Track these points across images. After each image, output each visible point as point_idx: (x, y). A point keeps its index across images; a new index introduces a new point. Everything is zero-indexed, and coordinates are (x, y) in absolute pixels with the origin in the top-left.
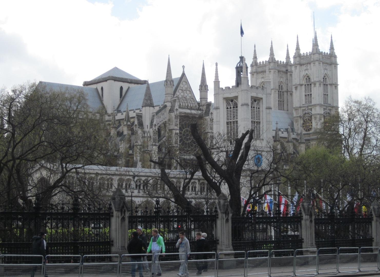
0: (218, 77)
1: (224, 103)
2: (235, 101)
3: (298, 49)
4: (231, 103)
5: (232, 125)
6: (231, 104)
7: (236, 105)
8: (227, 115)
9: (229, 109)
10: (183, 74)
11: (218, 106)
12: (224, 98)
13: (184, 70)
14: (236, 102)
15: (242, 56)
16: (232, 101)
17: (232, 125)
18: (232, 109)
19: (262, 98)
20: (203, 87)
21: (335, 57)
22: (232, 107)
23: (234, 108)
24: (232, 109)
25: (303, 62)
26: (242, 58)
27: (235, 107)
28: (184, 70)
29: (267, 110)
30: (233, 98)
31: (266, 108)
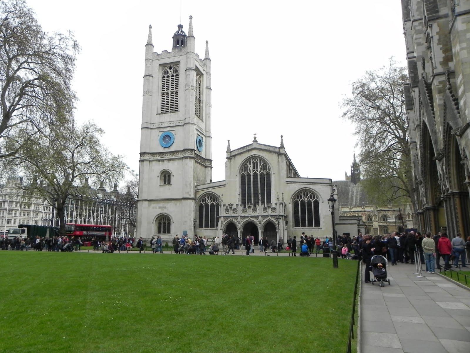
1: (159, 69)
4: (169, 70)
5: (170, 97)
6: (169, 72)
9: (166, 78)
11: (150, 73)
12: (160, 65)
15: (182, 24)
16: (170, 68)
17: (170, 97)
18: (170, 78)
19: (203, 75)
22: (170, 75)
23: (173, 76)
24: (170, 78)
26: (180, 27)
29: (207, 89)
31: (206, 88)
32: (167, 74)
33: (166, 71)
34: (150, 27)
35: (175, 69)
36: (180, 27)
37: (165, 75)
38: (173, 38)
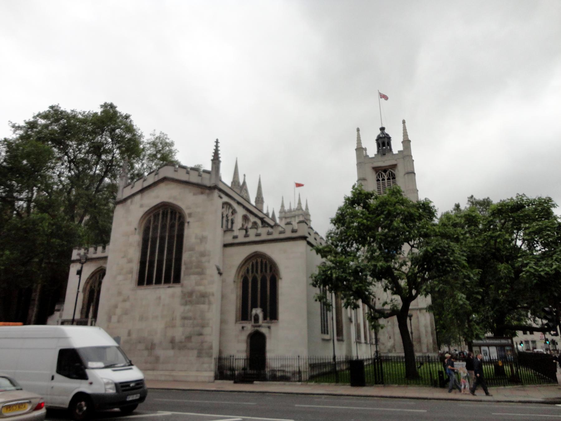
0: (361, 143)
2: (390, 171)
3: (283, 206)
4: (384, 174)
7: (392, 175)
8: (378, 189)
10: (244, 183)
13: (244, 178)
14: (392, 173)
15: (383, 126)
16: (385, 171)
18: (386, 180)
20: (260, 199)
21: (310, 215)
22: (386, 178)
23: (389, 179)
24: (386, 180)
25: (287, 215)
26: (382, 129)
27: (391, 178)
28: (244, 178)
30: (388, 167)
32: (382, 177)
33: (380, 174)
34: (358, 130)
35: (390, 173)
36: (382, 129)
37: (379, 177)
38: (377, 140)
